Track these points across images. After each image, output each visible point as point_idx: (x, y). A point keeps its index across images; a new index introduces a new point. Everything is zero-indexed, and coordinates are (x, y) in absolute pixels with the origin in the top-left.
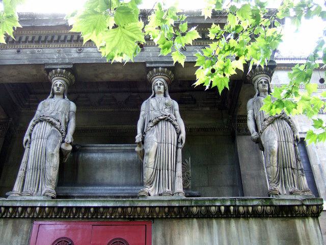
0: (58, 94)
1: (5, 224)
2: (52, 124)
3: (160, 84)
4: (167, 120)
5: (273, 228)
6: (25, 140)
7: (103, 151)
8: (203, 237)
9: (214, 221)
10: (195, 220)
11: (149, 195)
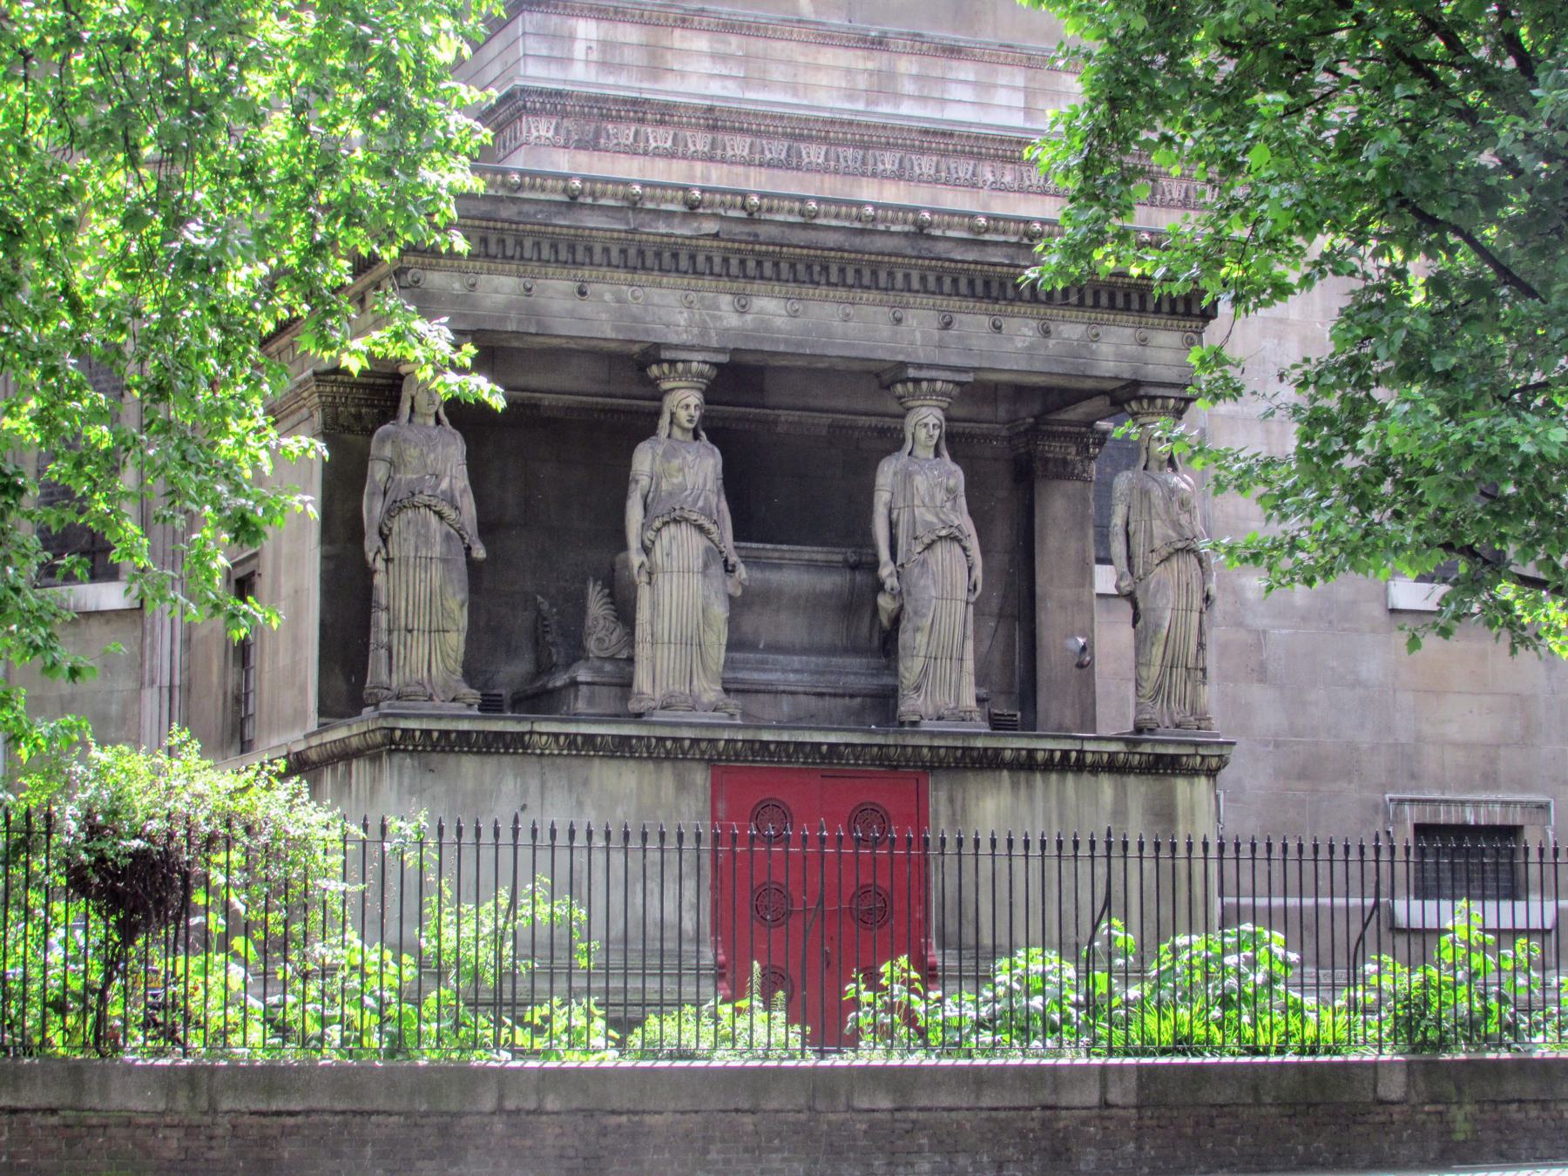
10: (1005, 773)
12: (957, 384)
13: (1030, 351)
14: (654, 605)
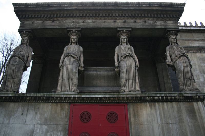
0: (74, 43)
1: (57, 105)
2: (73, 57)
3: (125, 38)
4: (130, 56)
5: (184, 106)
6: (60, 65)
7: (96, 71)
8: (152, 111)
9: (157, 103)
10: (148, 103)
11: (125, 91)
12: (128, 30)
13: (142, 25)
14: (63, 73)
